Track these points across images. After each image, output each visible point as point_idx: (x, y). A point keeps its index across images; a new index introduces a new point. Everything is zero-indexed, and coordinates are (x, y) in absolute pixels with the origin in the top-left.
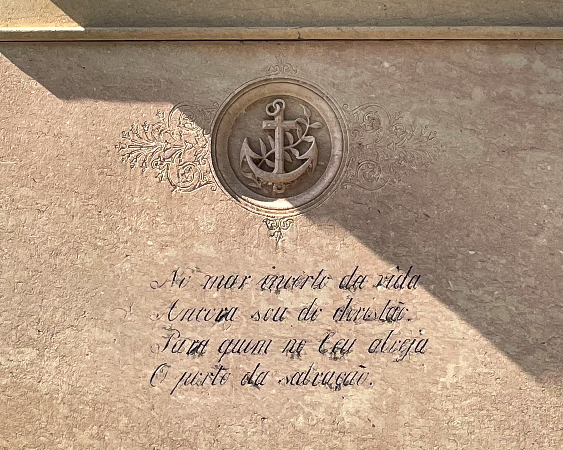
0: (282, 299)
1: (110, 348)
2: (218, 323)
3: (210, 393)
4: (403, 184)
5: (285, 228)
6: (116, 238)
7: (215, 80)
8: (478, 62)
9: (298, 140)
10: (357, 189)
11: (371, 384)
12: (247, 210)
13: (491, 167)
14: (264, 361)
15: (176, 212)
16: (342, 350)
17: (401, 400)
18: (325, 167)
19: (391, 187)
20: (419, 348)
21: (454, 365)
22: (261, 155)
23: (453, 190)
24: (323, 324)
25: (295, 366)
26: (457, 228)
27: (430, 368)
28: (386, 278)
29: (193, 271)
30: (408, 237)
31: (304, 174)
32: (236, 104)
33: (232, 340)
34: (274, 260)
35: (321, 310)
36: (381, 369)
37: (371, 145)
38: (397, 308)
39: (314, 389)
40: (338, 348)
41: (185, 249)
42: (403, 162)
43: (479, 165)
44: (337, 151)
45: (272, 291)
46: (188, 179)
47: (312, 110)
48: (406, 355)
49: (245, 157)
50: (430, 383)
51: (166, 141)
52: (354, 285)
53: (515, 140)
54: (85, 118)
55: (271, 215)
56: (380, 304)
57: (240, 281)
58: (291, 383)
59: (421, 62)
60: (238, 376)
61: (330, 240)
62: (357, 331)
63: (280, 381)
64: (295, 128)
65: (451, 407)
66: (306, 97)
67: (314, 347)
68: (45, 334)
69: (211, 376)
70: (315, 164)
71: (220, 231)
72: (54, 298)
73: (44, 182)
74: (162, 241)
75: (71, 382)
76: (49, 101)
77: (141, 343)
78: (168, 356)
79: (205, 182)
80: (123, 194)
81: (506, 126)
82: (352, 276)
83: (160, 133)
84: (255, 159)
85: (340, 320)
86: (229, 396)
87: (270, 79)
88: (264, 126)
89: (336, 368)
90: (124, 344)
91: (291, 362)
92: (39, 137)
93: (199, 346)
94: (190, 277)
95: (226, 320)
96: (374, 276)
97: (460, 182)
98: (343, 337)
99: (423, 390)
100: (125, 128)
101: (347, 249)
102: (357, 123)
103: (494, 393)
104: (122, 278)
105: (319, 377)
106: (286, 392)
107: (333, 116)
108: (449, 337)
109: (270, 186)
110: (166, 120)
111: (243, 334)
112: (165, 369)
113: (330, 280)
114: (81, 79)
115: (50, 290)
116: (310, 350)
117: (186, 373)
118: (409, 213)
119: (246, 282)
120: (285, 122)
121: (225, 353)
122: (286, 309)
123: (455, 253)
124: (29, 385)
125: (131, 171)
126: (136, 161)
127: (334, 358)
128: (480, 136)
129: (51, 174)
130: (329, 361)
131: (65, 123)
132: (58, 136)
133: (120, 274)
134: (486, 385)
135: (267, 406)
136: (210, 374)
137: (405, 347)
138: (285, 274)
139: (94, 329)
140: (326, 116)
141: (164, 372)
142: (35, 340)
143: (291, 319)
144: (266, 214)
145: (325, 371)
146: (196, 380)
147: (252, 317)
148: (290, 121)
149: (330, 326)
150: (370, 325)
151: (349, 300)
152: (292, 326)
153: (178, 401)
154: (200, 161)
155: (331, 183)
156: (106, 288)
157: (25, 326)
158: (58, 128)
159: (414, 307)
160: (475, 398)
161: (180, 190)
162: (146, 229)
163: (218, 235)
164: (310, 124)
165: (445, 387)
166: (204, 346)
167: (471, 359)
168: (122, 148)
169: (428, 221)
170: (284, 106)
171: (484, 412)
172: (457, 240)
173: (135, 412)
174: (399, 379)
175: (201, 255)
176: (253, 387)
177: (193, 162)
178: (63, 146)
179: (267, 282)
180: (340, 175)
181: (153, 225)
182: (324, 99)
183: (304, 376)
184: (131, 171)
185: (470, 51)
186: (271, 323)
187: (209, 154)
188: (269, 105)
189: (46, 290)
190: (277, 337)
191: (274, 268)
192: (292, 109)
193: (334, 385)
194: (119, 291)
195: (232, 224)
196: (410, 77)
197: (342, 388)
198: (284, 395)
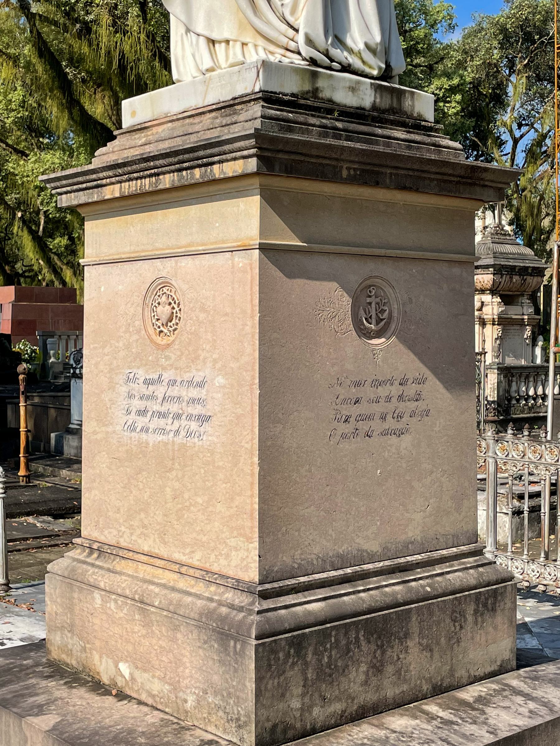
57: (363, 383)
62: (406, 407)
173: (323, 455)
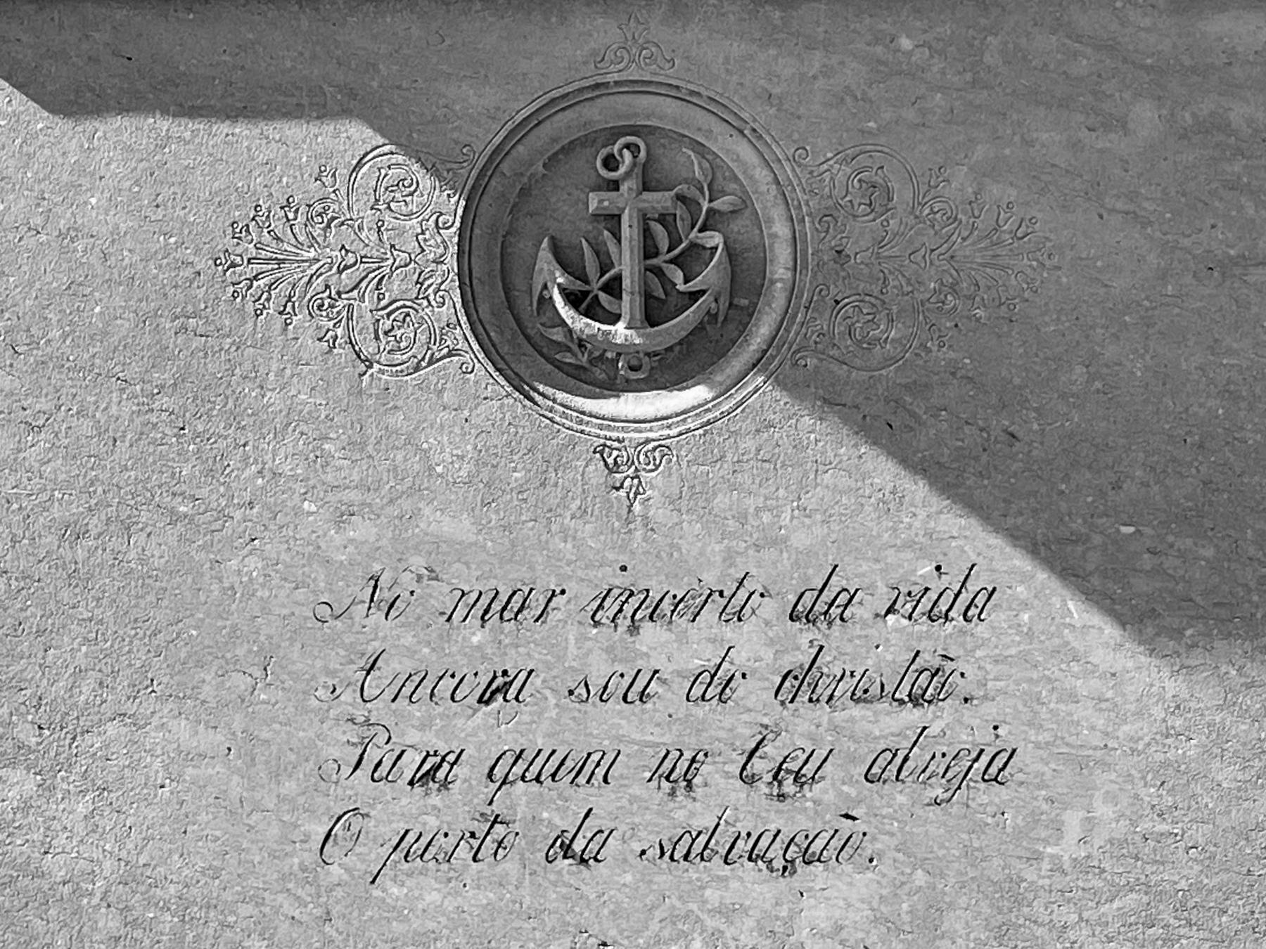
0: (644, 649)
1: (217, 769)
2: (485, 709)
3: (468, 882)
4: (952, 355)
5: (651, 467)
6: (223, 496)
7: (464, 88)
8: (1143, 35)
9: (681, 242)
10: (834, 367)
11: (871, 860)
12: (551, 420)
13: (1177, 310)
14: (603, 801)
15: (373, 432)
16: (797, 775)
17: (947, 899)
18: (751, 312)
19: (921, 362)
20: (993, 770)
21: (1082, 814)
22: (587, 282)
23: (1079, 369)
24: (750, 710)
25: (680, 815)
26: (1090, 468)
27: (1019, 821)
28: (909, 594)
29: (419, 578)
30: (962, 491)
31: (700, 329)
32: (520, 148)
33: (522, 751)
34: (623, 548)
35: (744, 676)
36: (896, 824)
37: (869, 253)
38: (938, 670)
39: (728, 873)
40: (788, 771)
41: (396, 522)
42: (949, 298)
43: (1146, 303)
44: (781, 271)
45: (619, 629)
46: (403, 345)
47: (714, 164)
48: (959, 788)
49: (545, 287)
50: (1020, 858)
51: (343, 247)
52: (826, 613)
53: (1240, 238)
54: (137, 189)
55: (614, 435)
56: (894, 662)
57: (538, 600)
58: (672, 858)
59: (996, 35)
60: (539, 839)
61: (766, 499)
62: (835, 729)
63: (643, 852)
64: (673, 211)
65: (1074, 917)
66: (699, 129)
67: (727, 768)
68: (56, 736)
69: (471, 841)
70: (723, 301)
71: (485, 476)
72: (75, 645)
73: (40, 353)
74: (340, 501)
75: (123, 854)
76: (41, 147)
77: (293, 757)
78: (361, 790)
79: (446, 350)
80: (238, 384)
81: (1217, 204)
82: (821, 591)
83: (329, 226)
84: (571, 293)
85: (792, 701)
86: (517, 888)
87: (606, 85)
88: (593, 206)
89: (782, 821)
90: (253, 760)
91: (671, 805)
92: (21, 239)
93: (440, 766)
94: (412, 593)
95: (505, 700)
96: (879, 591)
97: (1098, 349)
98: (800, 743)
99: (1001, 877)
100: (237, 214)
101: (807, 521)
102: (830, 197)
103: (1183, 884)
104: (243, 595)
105: (740, 843)
106: (656, 879)
107: (770, 179)
108: (1067, 744)
109: (612, 360)
110: (343, 191)
111: (548, 735)
112: (357, 823)
113: (766, 599)
114: (121, 89)
115: (63, 627)
116: (717, 776)
117: (407, 832)
118: (967, 429)
119: (552, 605)
120: (646, 195)
121: (504, 783)
122: (656, 672)
123: (1083, 530)
124: (19, 861)
125: (255, 325)
126: (268, 300)
127: (779, 796)
128: (1149, 230)
129: (55, 333)
130: (764, 802)
131: (86, 203)
132: (70, 234)
133: (236, 586)
134: (1163, 863)
135: (613, 913)
136: (468, 835)
137: (957, 769)
138: (652, 584)
139: (176, 722)
140: (751, 178)
141: (355, 829)
142: (30, 751)
143: (669, 698)
144: (602, 433)
145: (756, 827)
146: (432, 850)
147: (571, 692)
148: (660, 194)
149: (765, 715)
150: (869, 713)
151: (814, 651)
152: (670, 716)
153: (389, 901)
154: (431, 298)
155: (765, 351)
156: (203, 620)
157: (6, 716)
158: (68, 215)
159: (979, 668)
160: (1134, 896)
161: (381, 372)
162: (299, 471)
163: (481, 485)
164: (711, 201)
165: (1058, 869)
166: (452, 765)
167: (1125, 801)
168: (233, 265)
169: (1014, 449)
170: (643, 154)
171: (1157, 931)
172: (1090, 499)
173: (284, 927)
174: (942, 846)
175: (437, 537)
176: (574, 868)
177: (411, 300)
178: (84, 260)
179: (606, 604)
180: (788, 331)
181: (315, 462)
182: (745, 136)
183: (702, 840)
184: (255, 325)
185: (1124, 7)
186: (618, 707)
187: (452, 281)
188: (604, 152)
189: (53, 624)
190: (633, 742)
191: (624, 569)
192: (665, 161)
193: (778, 864)
194: (234, 628)
195: (515, 458)
196: (969, 76)
197: (799, 870)
198: (655, 887)
